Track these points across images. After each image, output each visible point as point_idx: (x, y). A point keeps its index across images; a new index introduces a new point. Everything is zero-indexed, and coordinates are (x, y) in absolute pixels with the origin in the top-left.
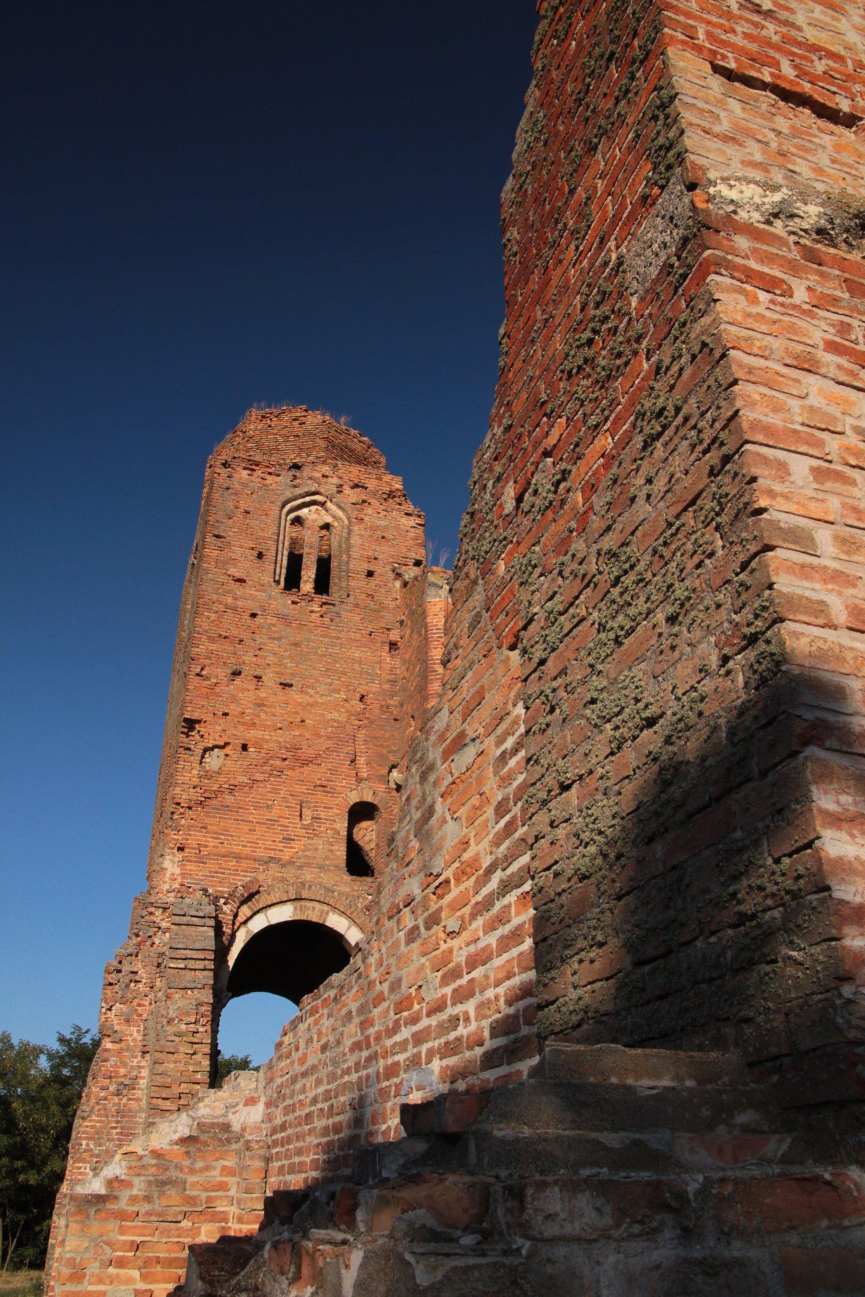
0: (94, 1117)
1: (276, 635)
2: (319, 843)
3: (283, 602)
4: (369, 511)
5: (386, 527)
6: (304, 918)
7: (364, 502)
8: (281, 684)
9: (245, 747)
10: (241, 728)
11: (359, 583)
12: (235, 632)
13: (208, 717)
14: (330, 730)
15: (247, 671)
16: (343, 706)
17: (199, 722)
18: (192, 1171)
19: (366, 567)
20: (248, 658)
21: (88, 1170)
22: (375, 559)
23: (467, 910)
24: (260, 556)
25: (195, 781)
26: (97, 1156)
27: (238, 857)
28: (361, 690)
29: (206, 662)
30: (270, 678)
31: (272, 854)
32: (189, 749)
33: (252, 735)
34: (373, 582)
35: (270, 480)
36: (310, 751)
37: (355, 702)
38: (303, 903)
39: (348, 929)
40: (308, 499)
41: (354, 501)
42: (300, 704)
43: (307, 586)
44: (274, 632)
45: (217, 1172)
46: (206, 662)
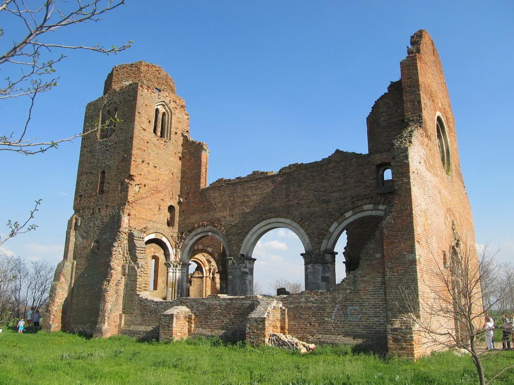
9: (145, 186)
12: (143, 148)
13: (136, 175)
15: (146, 161)
17: (133, 176)
24: (149, 122)
25: (133, 195)
27: (143, 219)
28: (172, 171)
30: (151, 165)
31: (151, 219)
33: (147, 182)
37: (171, 174)
40: (161, 103)
42: (158, 173)
43: (159, 134)
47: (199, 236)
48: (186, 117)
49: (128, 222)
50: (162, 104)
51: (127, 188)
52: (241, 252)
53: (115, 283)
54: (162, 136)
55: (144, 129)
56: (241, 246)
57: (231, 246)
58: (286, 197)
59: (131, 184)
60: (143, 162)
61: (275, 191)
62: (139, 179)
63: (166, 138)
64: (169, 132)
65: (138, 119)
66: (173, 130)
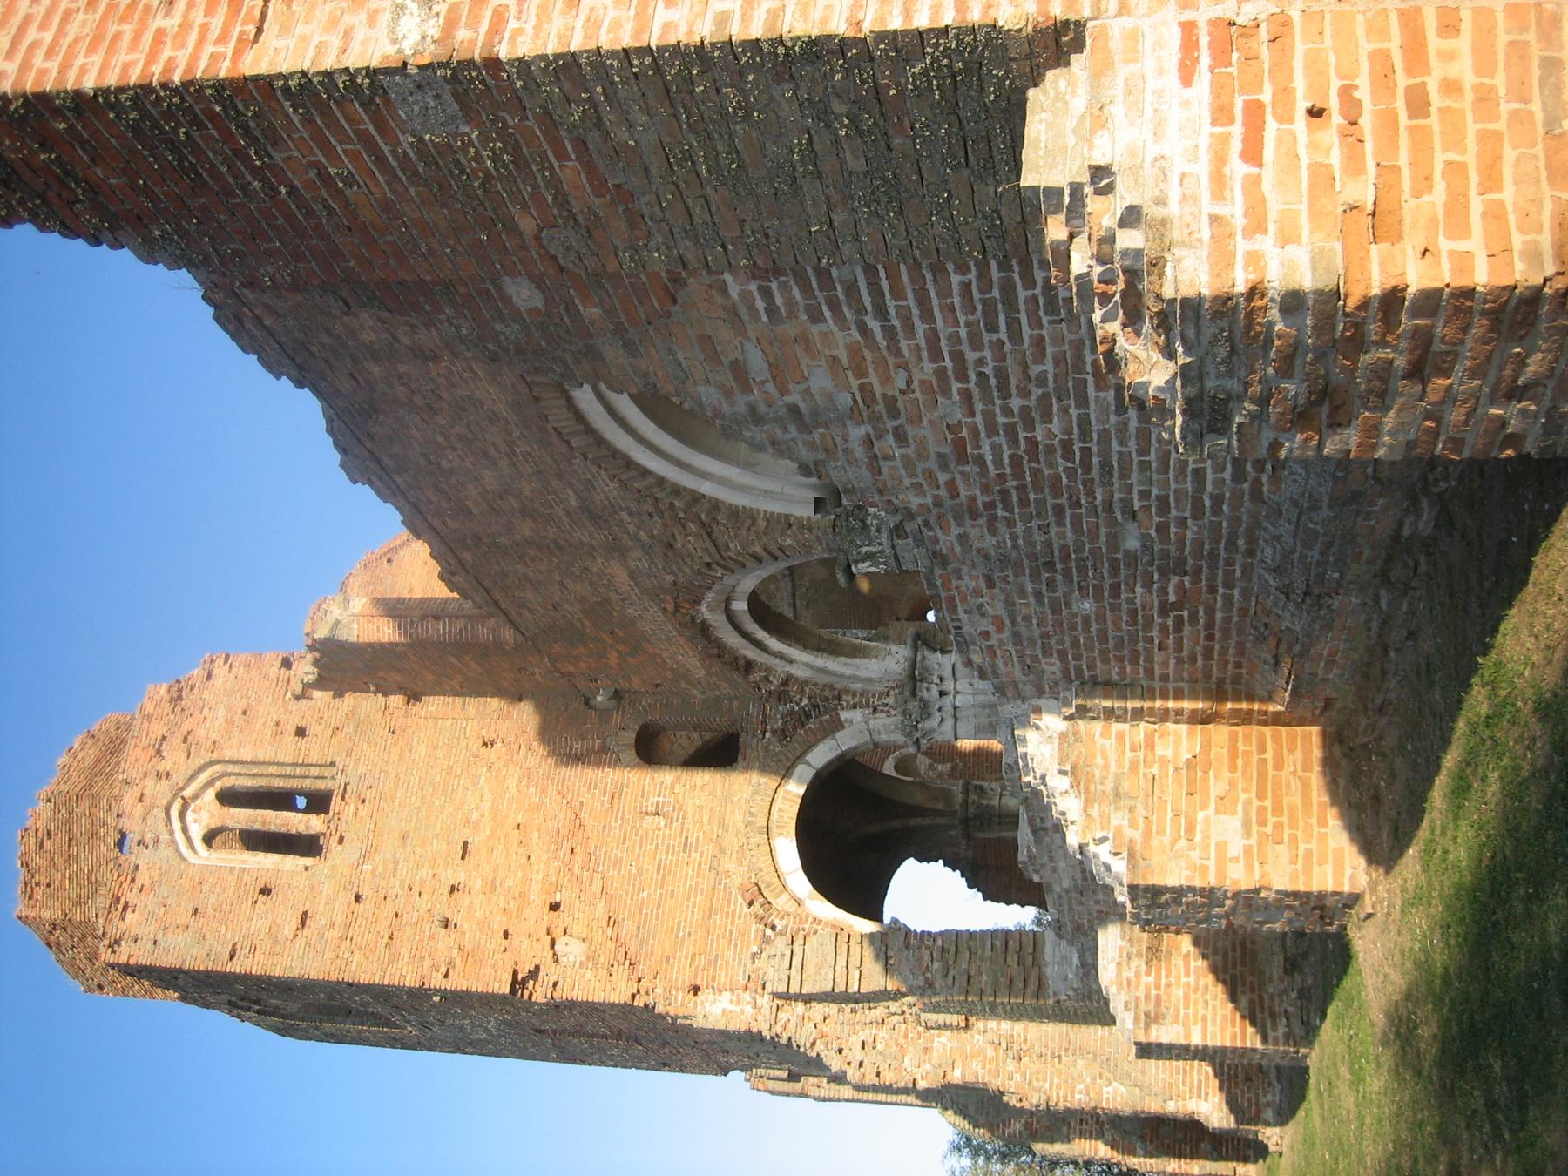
0: (1047, 1086)
1: (390, 866)
2: (690, 805)
3: (337, 857)
4: (201, 733)
5: (229, 709)
6: (793, 823)
7: (185, 740)
8: (463, 858)
9: (555, 907)
10: (527, 912)
11: (313, 750)
12: (384, 924)
13: (509, 960)
14: (532, 790)
15: (443, 907)
16: (499, 771)
17: (515, 973)
18: (1106, 767)
19: (289, 737)
20: (423, 904)
21: (1110, 1089)
22: (277, 724)
23: (891, 360)
24: (265, 891)
25: (602, 973)
26: (1094, 1079)
28: (476, 746)
29: (427, 964)
32: (555, 984)
33: (538, 898)
34: (313, 728)
35: (143, 878)
36: (561, 816)
38: (773, 825)
39: (809, 764)
40: (177, 824)
41: (184, 755)
43: (314, 824)
44: (385, 868)
45: (1107, 742)
46: (427, 964)
47: (761, 635)
48: (220, 669)
49: (727, 995)
50: (182, 815)
51: (572, 1005)
52: (805, 511)
53: (1011, 1066)
54: (319, 803)
55: (303, 923)
56: (770, 519)
57: (778, 553)
58: (436, 358)
59: (555, 984)
60: (446, 924)
61: (418, 400)
62: (526, 941)
63: (329, 785)
64: (298, 771)
65: (259, 957)
66: (288, 749)
